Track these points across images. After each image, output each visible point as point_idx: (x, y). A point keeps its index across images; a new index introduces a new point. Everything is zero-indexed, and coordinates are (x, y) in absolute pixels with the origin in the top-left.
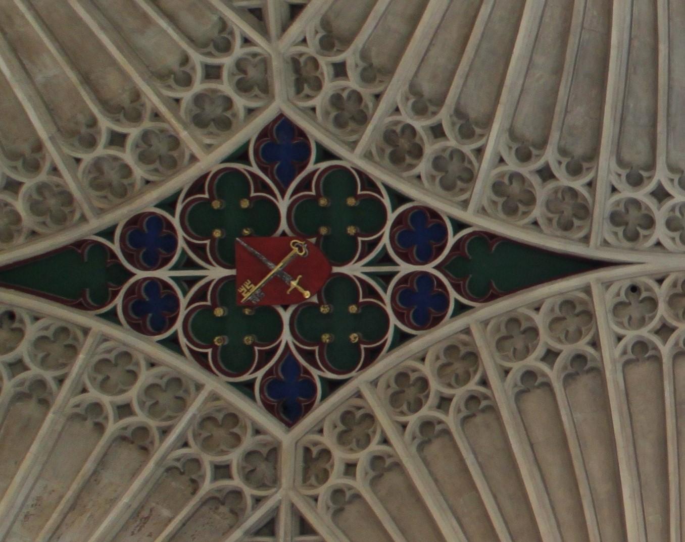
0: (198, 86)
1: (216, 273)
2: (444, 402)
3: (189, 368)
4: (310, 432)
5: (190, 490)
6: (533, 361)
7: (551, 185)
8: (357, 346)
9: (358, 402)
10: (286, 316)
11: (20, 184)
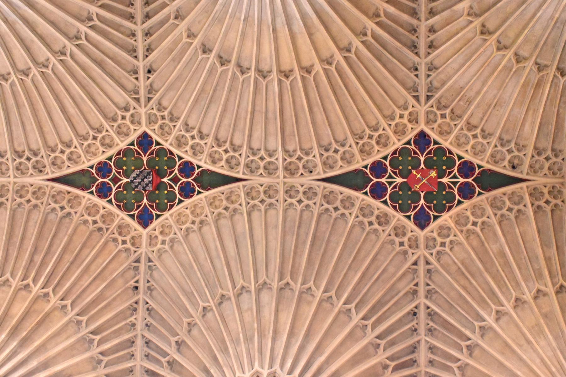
0: (447, 240)
1: (445, 180)
2: (370, 137)
3: (455, 150)
4: (415, 129)
5: (454, 110)
6: (342, 150)
7: (335, 206)
8: (400, 156)
9: (399, 138)
10: (422, 166)
11: (507, 210)
